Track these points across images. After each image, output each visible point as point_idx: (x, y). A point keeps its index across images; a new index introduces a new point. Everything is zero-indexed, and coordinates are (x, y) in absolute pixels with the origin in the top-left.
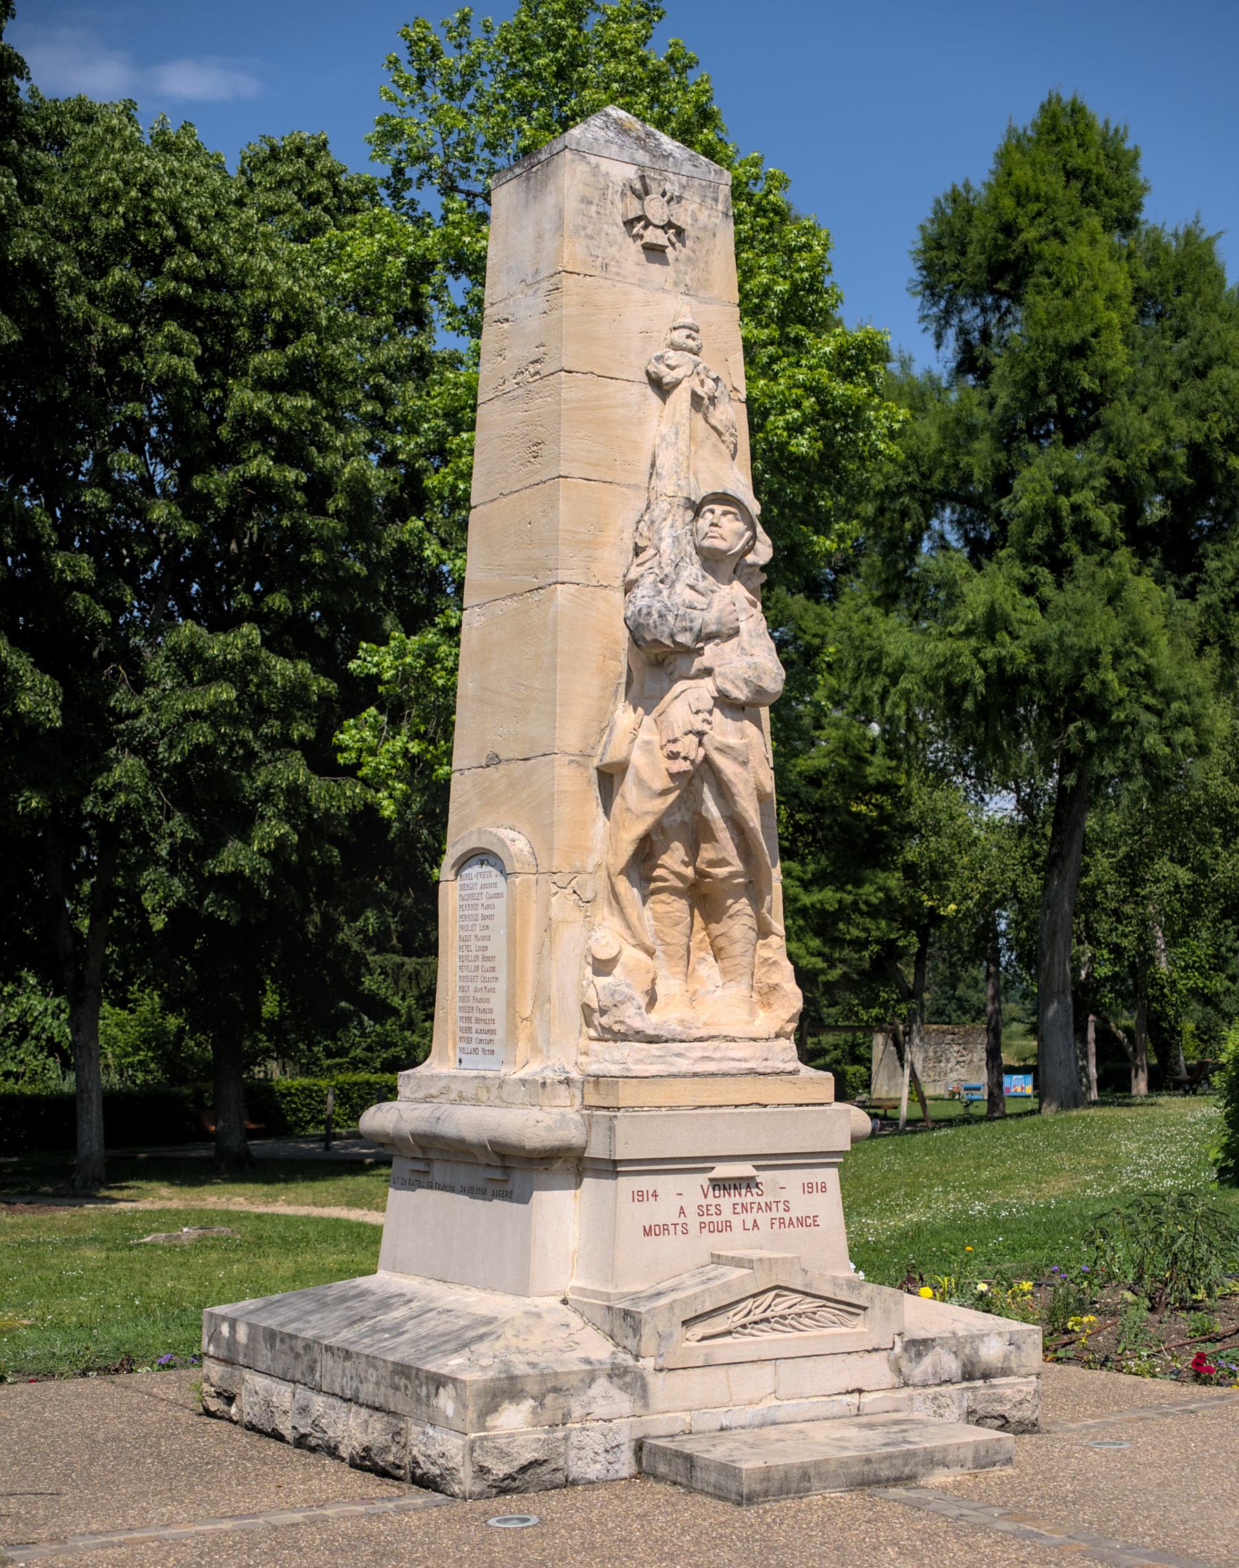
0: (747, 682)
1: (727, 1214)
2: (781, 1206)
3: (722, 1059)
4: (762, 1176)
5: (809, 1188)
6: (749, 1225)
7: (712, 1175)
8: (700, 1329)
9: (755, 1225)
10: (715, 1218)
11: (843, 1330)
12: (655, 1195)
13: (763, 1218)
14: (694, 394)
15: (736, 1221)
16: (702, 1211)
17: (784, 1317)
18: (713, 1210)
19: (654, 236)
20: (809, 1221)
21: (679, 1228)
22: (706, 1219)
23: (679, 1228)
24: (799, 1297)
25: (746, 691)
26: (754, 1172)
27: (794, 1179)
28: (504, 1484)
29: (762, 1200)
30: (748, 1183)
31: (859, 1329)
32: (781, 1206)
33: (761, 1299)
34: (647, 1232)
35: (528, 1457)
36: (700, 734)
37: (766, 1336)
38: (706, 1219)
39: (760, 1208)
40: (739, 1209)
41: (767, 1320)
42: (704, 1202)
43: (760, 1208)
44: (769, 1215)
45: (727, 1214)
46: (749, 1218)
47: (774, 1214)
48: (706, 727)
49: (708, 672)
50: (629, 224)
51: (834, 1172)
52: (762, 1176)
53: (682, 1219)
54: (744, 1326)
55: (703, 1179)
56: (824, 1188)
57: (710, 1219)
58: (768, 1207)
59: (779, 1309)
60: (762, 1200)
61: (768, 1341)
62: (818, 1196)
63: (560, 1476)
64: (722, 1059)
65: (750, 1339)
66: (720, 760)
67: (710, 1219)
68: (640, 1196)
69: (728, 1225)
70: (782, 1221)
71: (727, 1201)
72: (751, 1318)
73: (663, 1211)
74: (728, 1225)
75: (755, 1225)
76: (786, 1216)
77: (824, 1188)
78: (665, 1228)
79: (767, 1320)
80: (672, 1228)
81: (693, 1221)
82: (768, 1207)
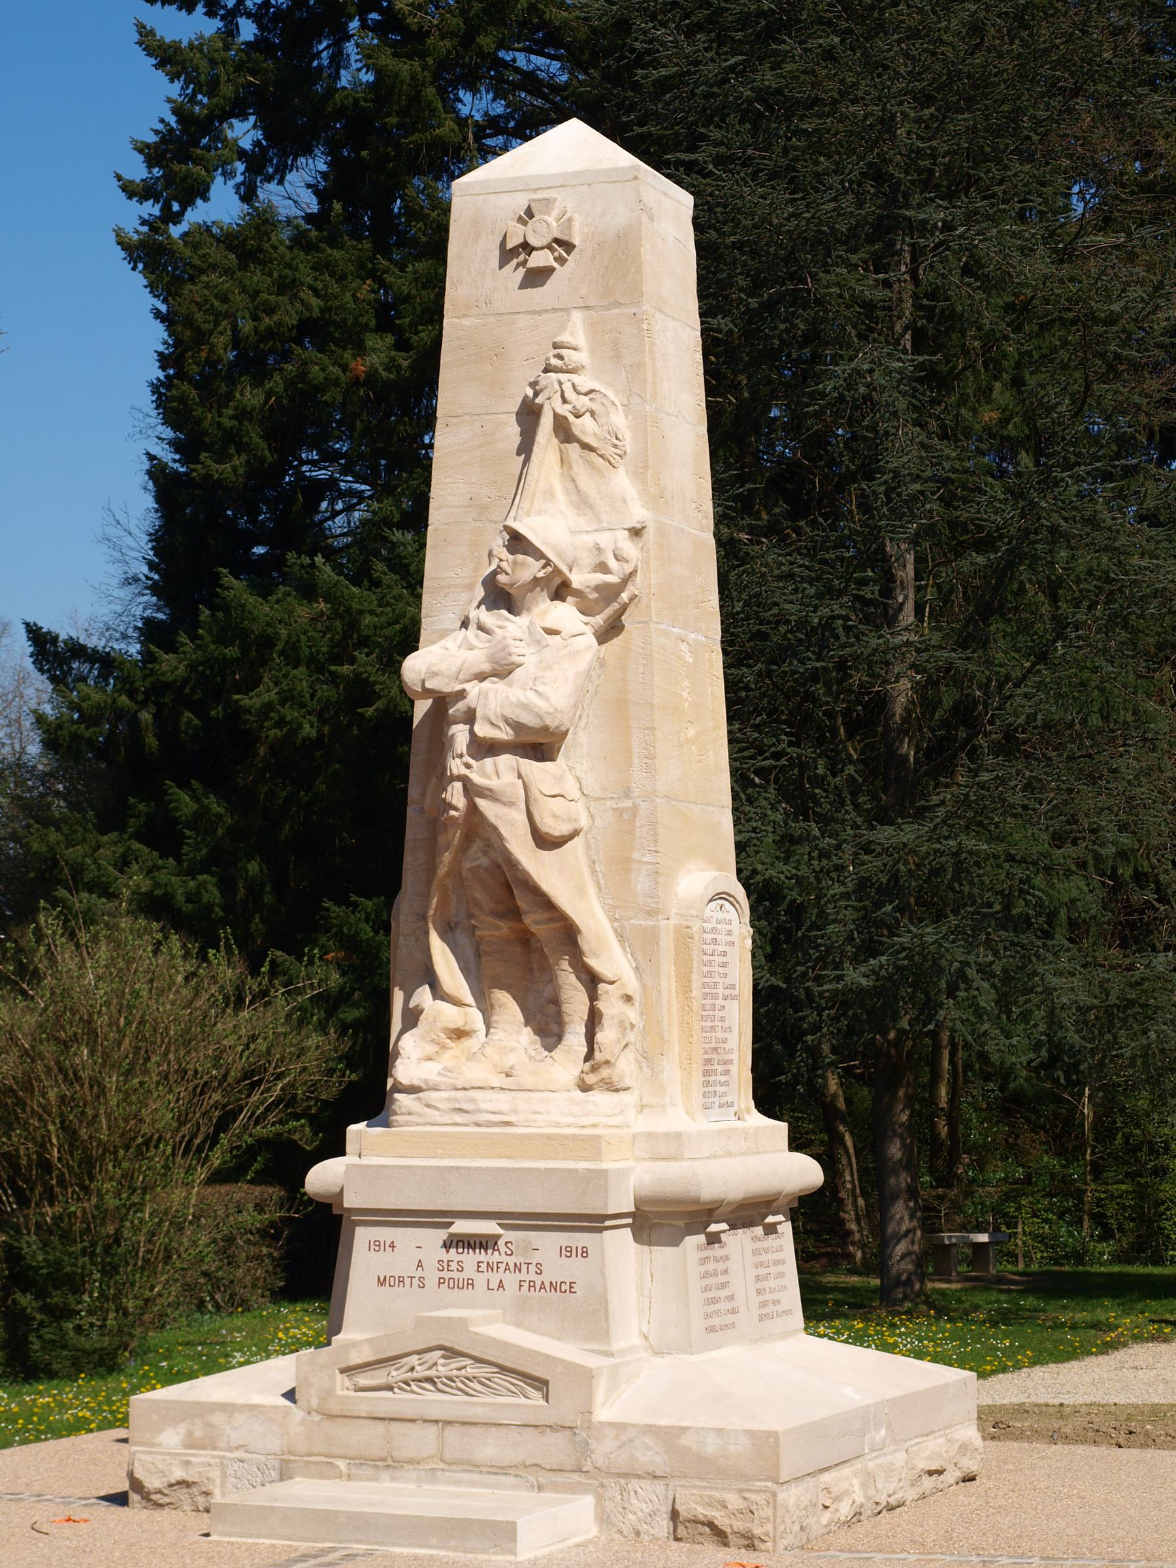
0: (507, 721)
1: (469, 1271)
2: (533, 1268)
5: (568, 1252)
6: (494, 1284)
8: (363, 1380)
9: (501, 1285)
10: (456, 1275)
11: (523, 1400)
12: (392, 1246)
13: (511, 1280)
15: (480, 1280)
16: (444, 1266)
17: (450, 1379)
18: (454, 1266)
19: (539, 259)
20: (564, 1287)
21: (416, 1281)
22: (446, 1274)
23: (416, 1281)
27: (549, 1242)
29: (511, 1261)
32: (533, 1268)
33: (427, 1356)
34: (382, 1282)
35: (178, 1474)
38: (446, 1274)
40: (483, 1267)
43: (507, 1269)
45: (469, 1271)
46: (495, 1278)
47: (523, 1275)
53: (419, 1273)
55: (443, 1234)
57: (451, 1275)
58: (517, 1268)
60: (511, 1261)
61: (432, 1401)
62: (577, 1262)
67: (451, 1275)
68: (377, 1246)
69: (471, 1283)
70: (532, 1284)
71: (470, 1258)
72: (415, 1375)
73: (400, 1262)
74: (471, 1283)
75: (501, 1285)
78: (401, 1280)
80: (407, 1281)
82: (517, 1268)
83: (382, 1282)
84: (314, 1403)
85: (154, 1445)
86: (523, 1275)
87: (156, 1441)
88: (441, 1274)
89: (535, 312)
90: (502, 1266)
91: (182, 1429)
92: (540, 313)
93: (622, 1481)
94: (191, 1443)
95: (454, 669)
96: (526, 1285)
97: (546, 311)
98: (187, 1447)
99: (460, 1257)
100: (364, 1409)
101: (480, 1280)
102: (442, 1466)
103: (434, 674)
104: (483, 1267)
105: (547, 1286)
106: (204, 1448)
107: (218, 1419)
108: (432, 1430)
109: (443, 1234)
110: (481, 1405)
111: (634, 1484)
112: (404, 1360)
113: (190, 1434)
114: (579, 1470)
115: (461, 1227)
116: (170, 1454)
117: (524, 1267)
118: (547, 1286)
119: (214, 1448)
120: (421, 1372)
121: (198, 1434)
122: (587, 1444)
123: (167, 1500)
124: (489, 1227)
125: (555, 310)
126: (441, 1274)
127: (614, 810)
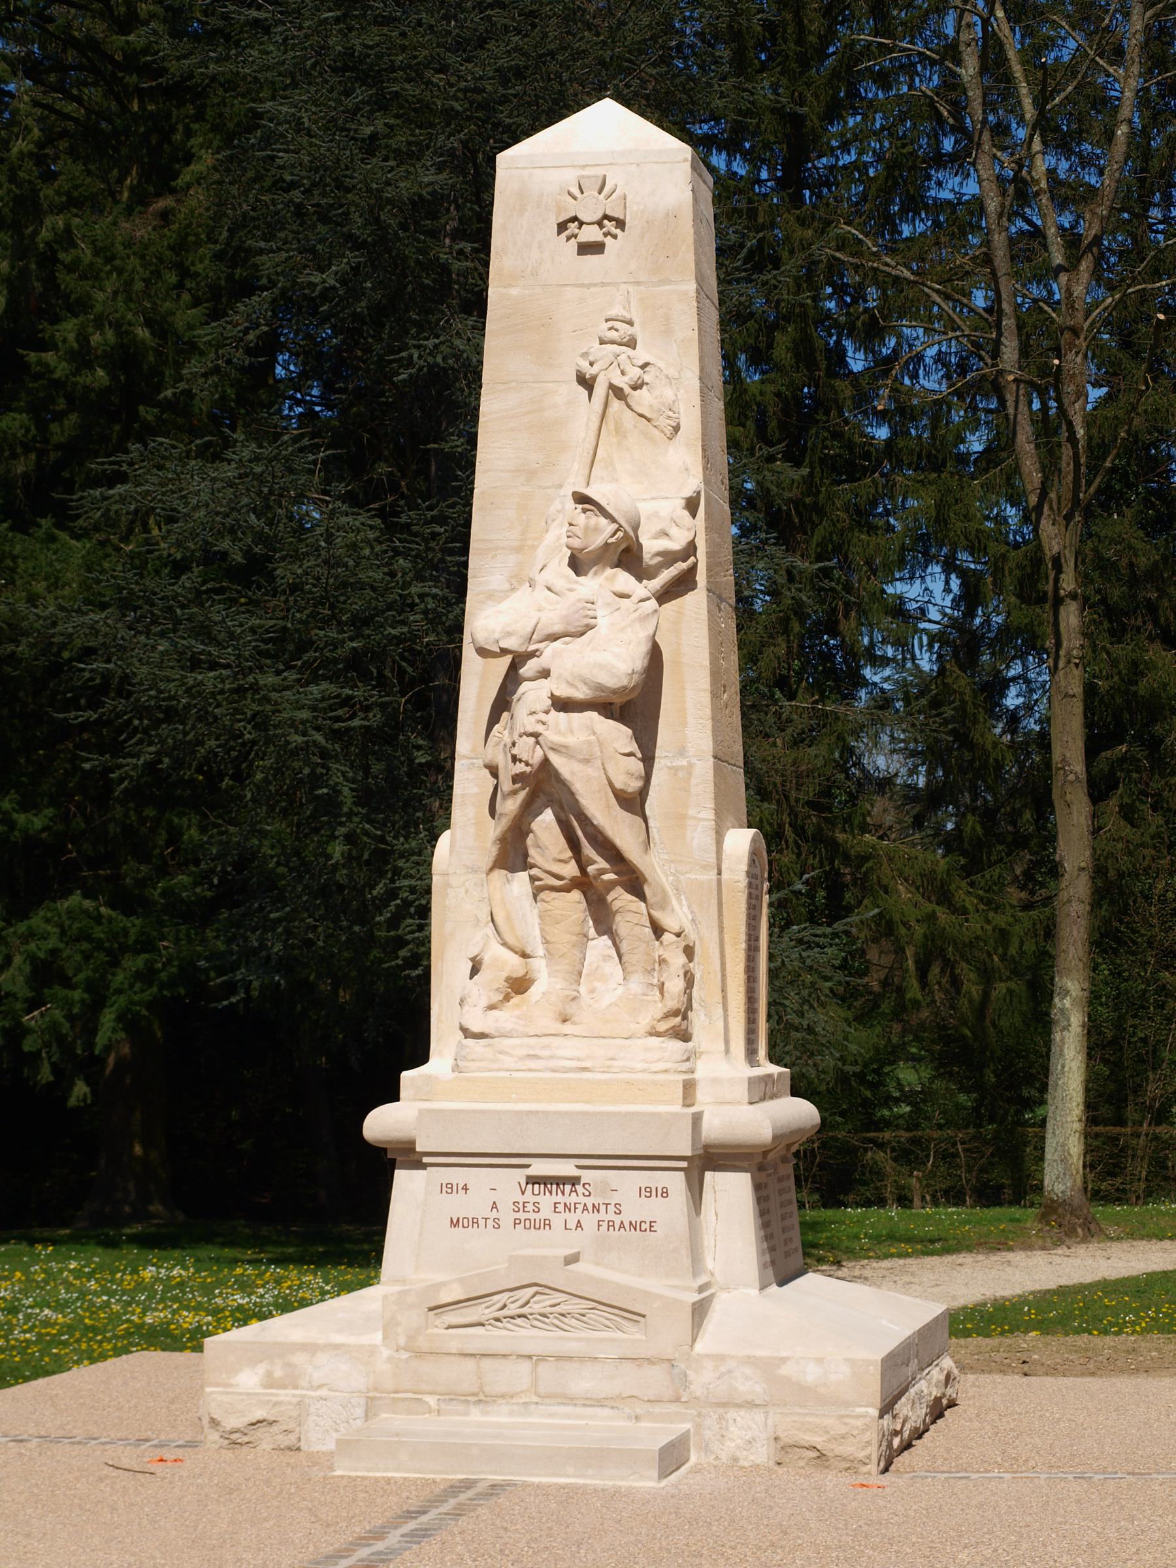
1: (546, 1212)
2: (611, 1208)
3: (551, 1057)
4: (587, 1176)
5: (648, 1192)
6: (572, 1224)
7: (530, 1172)
9: (579, 1225)
10: (532, 1216)
11: (619, 1335)
12: (465, 1188)
13: (589, 1220)
14: (612, 387)
15: (557, 1220)
18: (530, 1207)
19: (591, 234)
21: (490, 1223)
22: (522, 1215)
23: (490, 1223)
24: (564, 1297)
25: (584, 689)
26: (575, 1172)
27: (628, 1182)
28: (234, 1436)
30: (574, 1181)
31: (638, 1336)
32: (611, 1208)
34: (455, 1223)
35: (259, 1414)
36: (536, 735)
37: (523, 1332)
38: (522, 1215)
39: (585, 1208)
40: (560, 1208)
41: (524, 1316)
42: (521, 1199)
43: (585, 1208)
44: (597, 1216)
45: (546, 1212)
46: (572, 1219)
48: (540, 728)
49: (545, 674)
50: (562, 227)
51: (681, 1175)
52: (587, 1176)
53: (494, 1214)
54: (498, 1320)
55: (520, 1175)
56: (665, 1193)
57: (526, 1215)
59: (536, 1307)
60: (589, 1202)
61: (526, 1337)
63: (291, 1439)
64: (551, 1057)
65: (505, 1332)
66: (556, 760)
67: (526, 1215)
68: (450, 1188)
69: (547, 1224)
70: (611, 1225)
71: (547, 1200)
73: (474, 1204)
74: (547, 1224)
75: (579, 1225)
76: (617, 1220)
77: (665, 1193)
78: (475, 1221)
79: (524, 1316)
80: (481, 1222)
81: (507, 1216)
83: (455, 1223)
84: (402, 1341)
85: (232, 1385)
86: (602, 1215)
87: (233, 1381)
88: (517, 1215)
89: (582, 285)
90: (580, 1207)
91: (261, 1369)
92: (589, 286)
93: (721, 1410)
94: (270, 1382)
95: (529, 629)
96: (605, 1225)
97: (595, 285)
98: (266, 1387)
99: (536, 1199)
100: (454, 1346)
101: (557, 1220)
102: (536, 1399)
103: (509, 634)
104: (560, 1208)
105: (627, 1226)
106: (284, 1387)
107: (299, 1359)
108: (526, 1366)
109: (520, 1175)
110: (574, 1340)
111: (732, 1414)
112: (496, 1298)
113: (269, 1374)
114: (677, 1400)
115: (540, 1168)
116: (248, 1394)
117: (603, 1208)
118: (627, 1226)
119: (296, 1387)
120: (512, 1310)
121: (278, 1373)
122: (686, 1375)
123: (246, 1439)
124: (566, 1168)
125: (603, 284)
126: (517, 1215)
127: (669, 768)
